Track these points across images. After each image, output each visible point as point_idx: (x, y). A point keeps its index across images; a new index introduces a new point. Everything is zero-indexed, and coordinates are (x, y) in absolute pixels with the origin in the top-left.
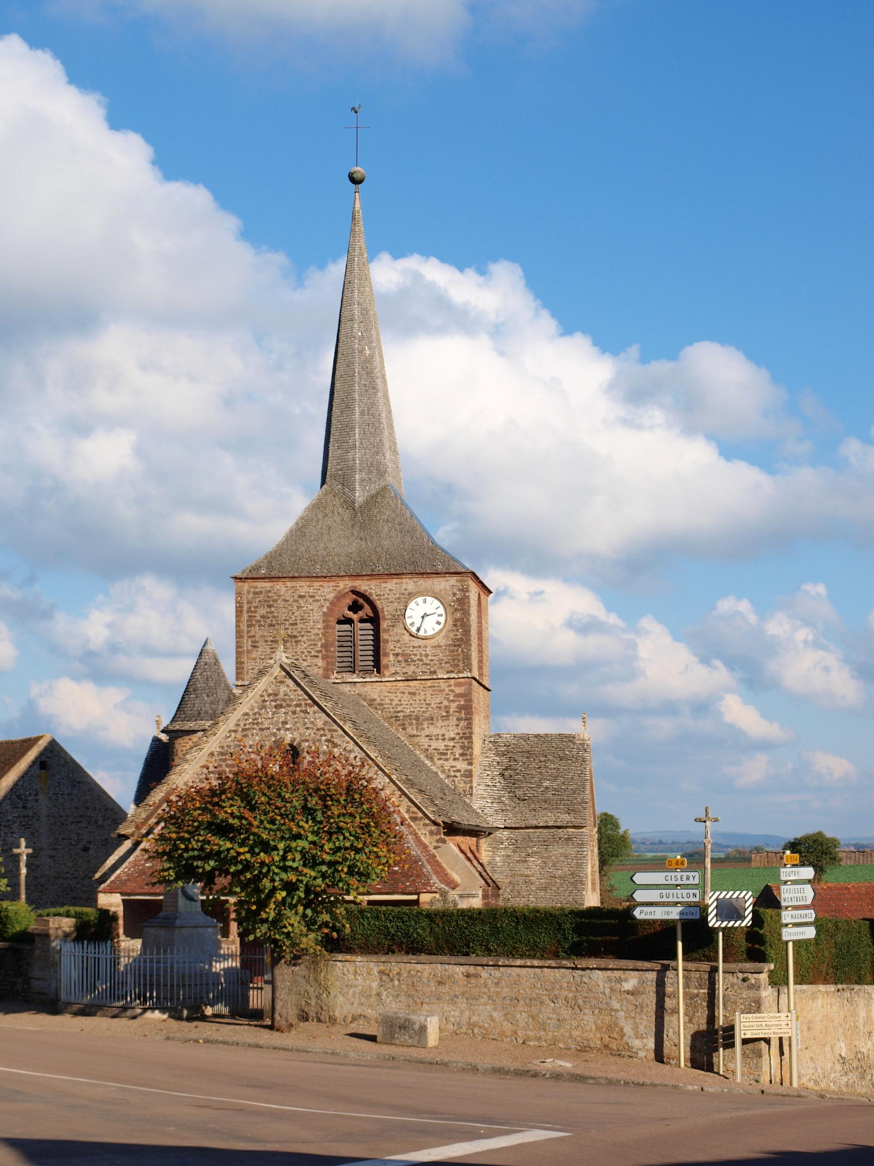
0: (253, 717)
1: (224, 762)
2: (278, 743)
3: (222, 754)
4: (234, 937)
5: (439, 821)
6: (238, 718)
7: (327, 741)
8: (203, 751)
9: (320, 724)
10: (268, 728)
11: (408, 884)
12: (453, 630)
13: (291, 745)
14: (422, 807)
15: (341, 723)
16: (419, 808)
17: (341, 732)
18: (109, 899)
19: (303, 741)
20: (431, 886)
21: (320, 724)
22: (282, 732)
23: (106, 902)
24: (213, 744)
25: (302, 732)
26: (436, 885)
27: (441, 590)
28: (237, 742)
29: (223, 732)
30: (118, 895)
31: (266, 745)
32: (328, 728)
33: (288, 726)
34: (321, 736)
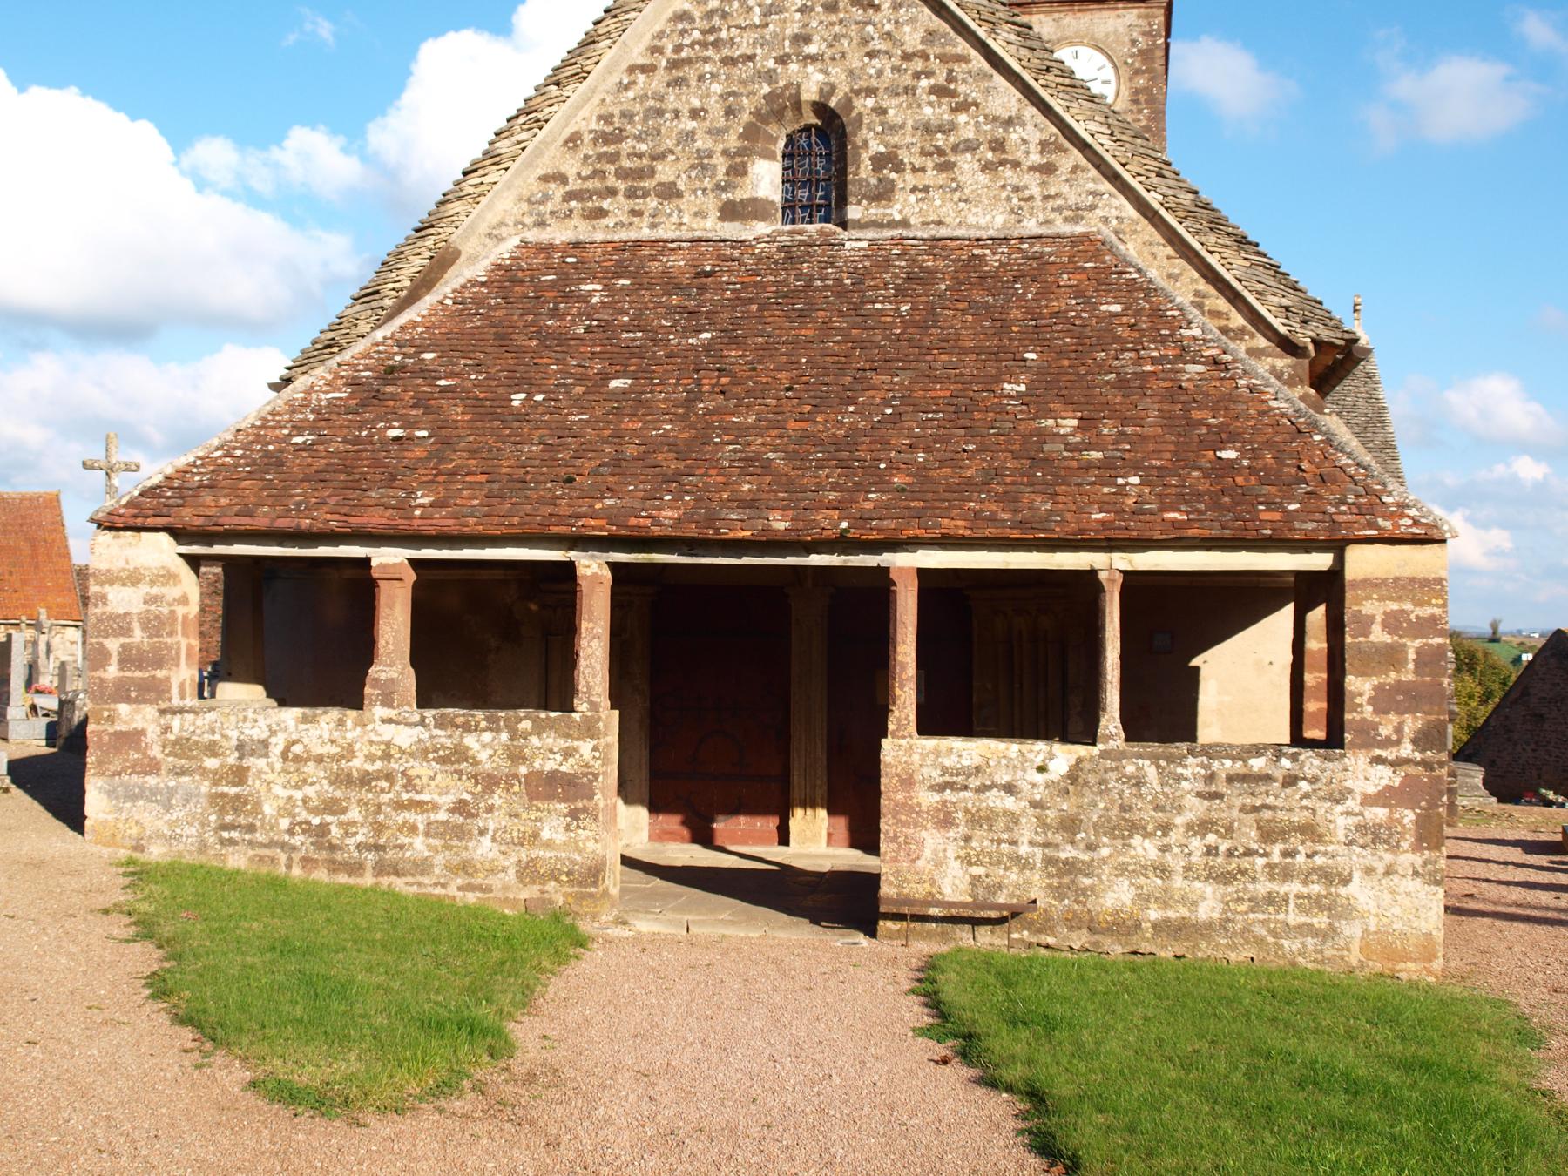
0: (705, 25)
1: (612, 162)
2: (782, 104)
3: (606, 138)
4: (594, 706)
5: (1304, 337)
6: (657, 28)
7: (933, 90)
8: (547, 127)
9: (912, 38)
10: (751, 58)
11: (1292, 507)
12: (1132, 111)
13: (820, 108)
14: (1246, 294)
15: (981, 32)
16: (1235, 298)
17: (979, 62)
18: (130, 552)
19: (857, 93)
20: (1386, 517)
21: (912, 38)
22: (793, 67)
23: (120, 564)
24: (578, 107)
25: (856, 64)
26: (1413, 512)
27: (1107, 35)
28: (651, 103)
29: (609, 71)
30: (164, 538)
31: (742, 109)
32: (938, 50)
33: (812, 49)
34: (917, 76)
